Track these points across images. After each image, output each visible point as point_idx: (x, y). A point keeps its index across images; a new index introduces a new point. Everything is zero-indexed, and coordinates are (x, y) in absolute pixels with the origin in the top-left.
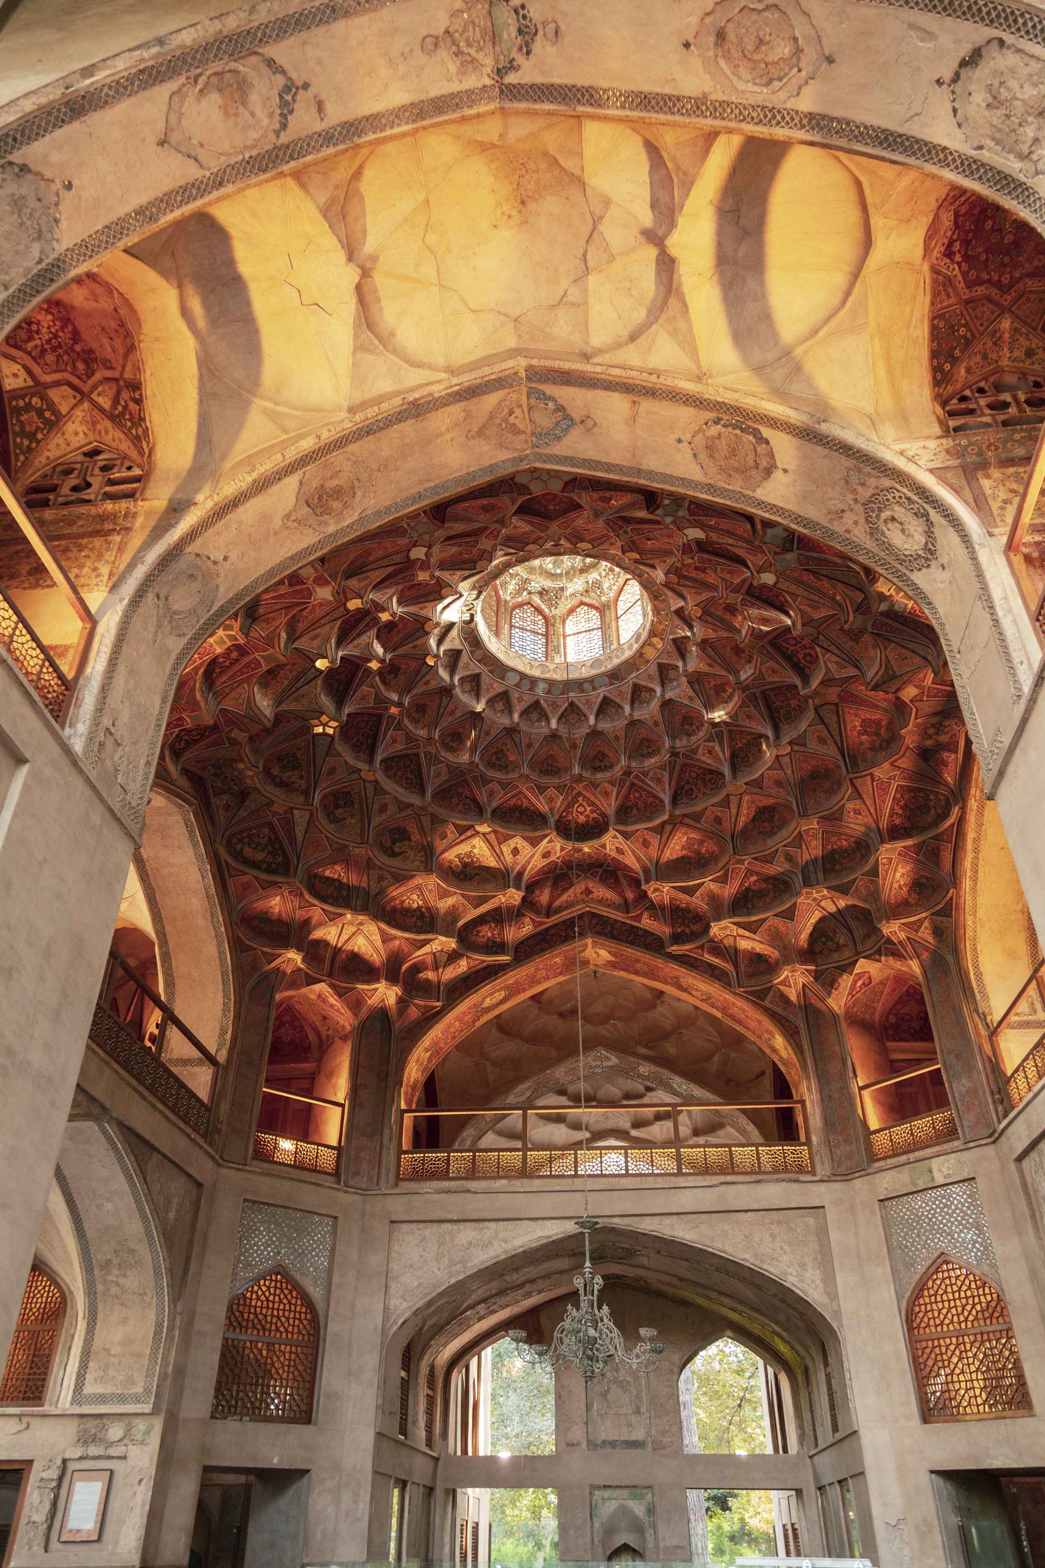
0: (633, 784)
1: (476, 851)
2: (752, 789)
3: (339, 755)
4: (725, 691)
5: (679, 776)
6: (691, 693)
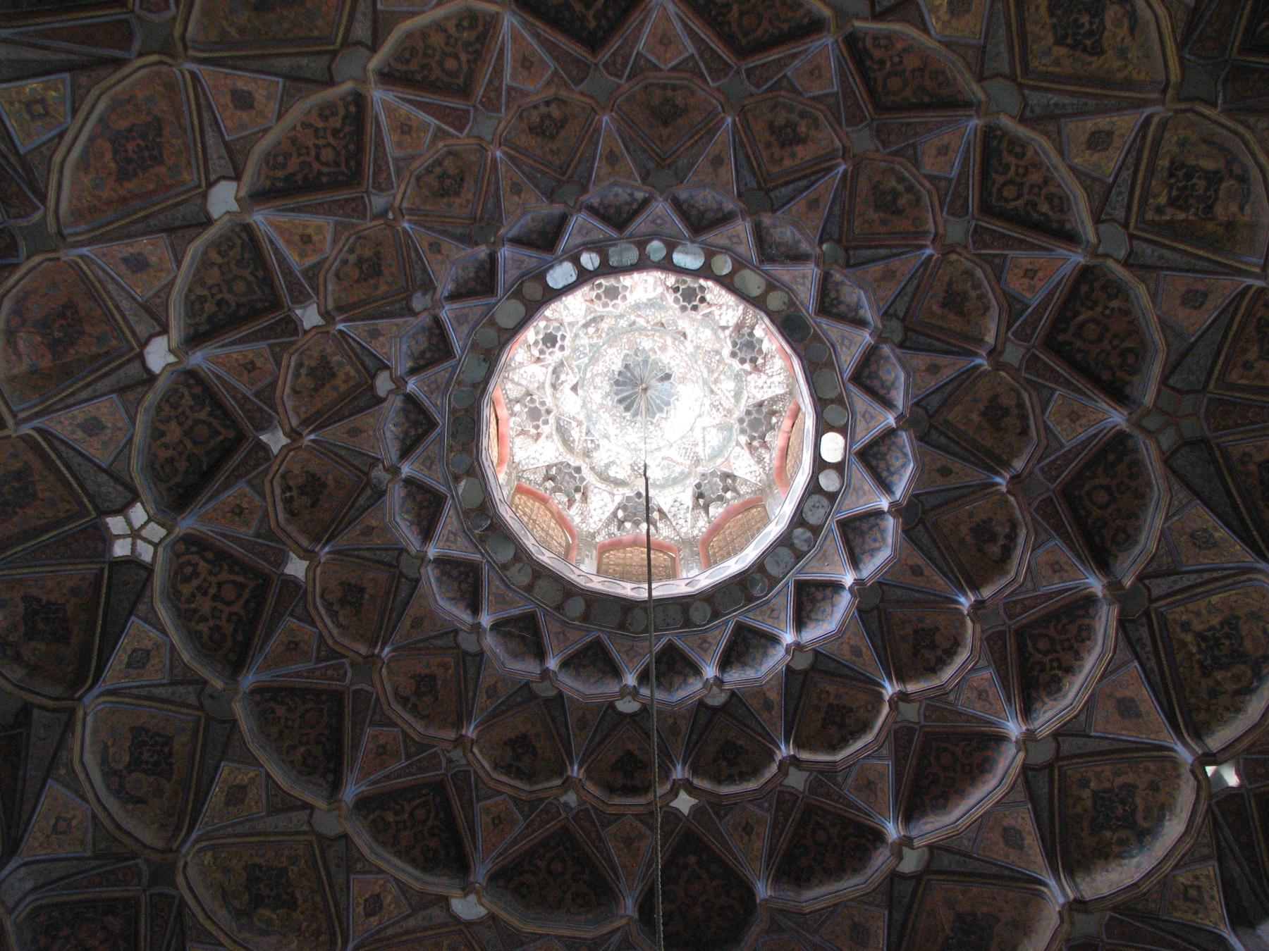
0: (465, 92)
3: (1161, 321)
4: (312, 372)
5: (360, 149)
6: (377, 347)
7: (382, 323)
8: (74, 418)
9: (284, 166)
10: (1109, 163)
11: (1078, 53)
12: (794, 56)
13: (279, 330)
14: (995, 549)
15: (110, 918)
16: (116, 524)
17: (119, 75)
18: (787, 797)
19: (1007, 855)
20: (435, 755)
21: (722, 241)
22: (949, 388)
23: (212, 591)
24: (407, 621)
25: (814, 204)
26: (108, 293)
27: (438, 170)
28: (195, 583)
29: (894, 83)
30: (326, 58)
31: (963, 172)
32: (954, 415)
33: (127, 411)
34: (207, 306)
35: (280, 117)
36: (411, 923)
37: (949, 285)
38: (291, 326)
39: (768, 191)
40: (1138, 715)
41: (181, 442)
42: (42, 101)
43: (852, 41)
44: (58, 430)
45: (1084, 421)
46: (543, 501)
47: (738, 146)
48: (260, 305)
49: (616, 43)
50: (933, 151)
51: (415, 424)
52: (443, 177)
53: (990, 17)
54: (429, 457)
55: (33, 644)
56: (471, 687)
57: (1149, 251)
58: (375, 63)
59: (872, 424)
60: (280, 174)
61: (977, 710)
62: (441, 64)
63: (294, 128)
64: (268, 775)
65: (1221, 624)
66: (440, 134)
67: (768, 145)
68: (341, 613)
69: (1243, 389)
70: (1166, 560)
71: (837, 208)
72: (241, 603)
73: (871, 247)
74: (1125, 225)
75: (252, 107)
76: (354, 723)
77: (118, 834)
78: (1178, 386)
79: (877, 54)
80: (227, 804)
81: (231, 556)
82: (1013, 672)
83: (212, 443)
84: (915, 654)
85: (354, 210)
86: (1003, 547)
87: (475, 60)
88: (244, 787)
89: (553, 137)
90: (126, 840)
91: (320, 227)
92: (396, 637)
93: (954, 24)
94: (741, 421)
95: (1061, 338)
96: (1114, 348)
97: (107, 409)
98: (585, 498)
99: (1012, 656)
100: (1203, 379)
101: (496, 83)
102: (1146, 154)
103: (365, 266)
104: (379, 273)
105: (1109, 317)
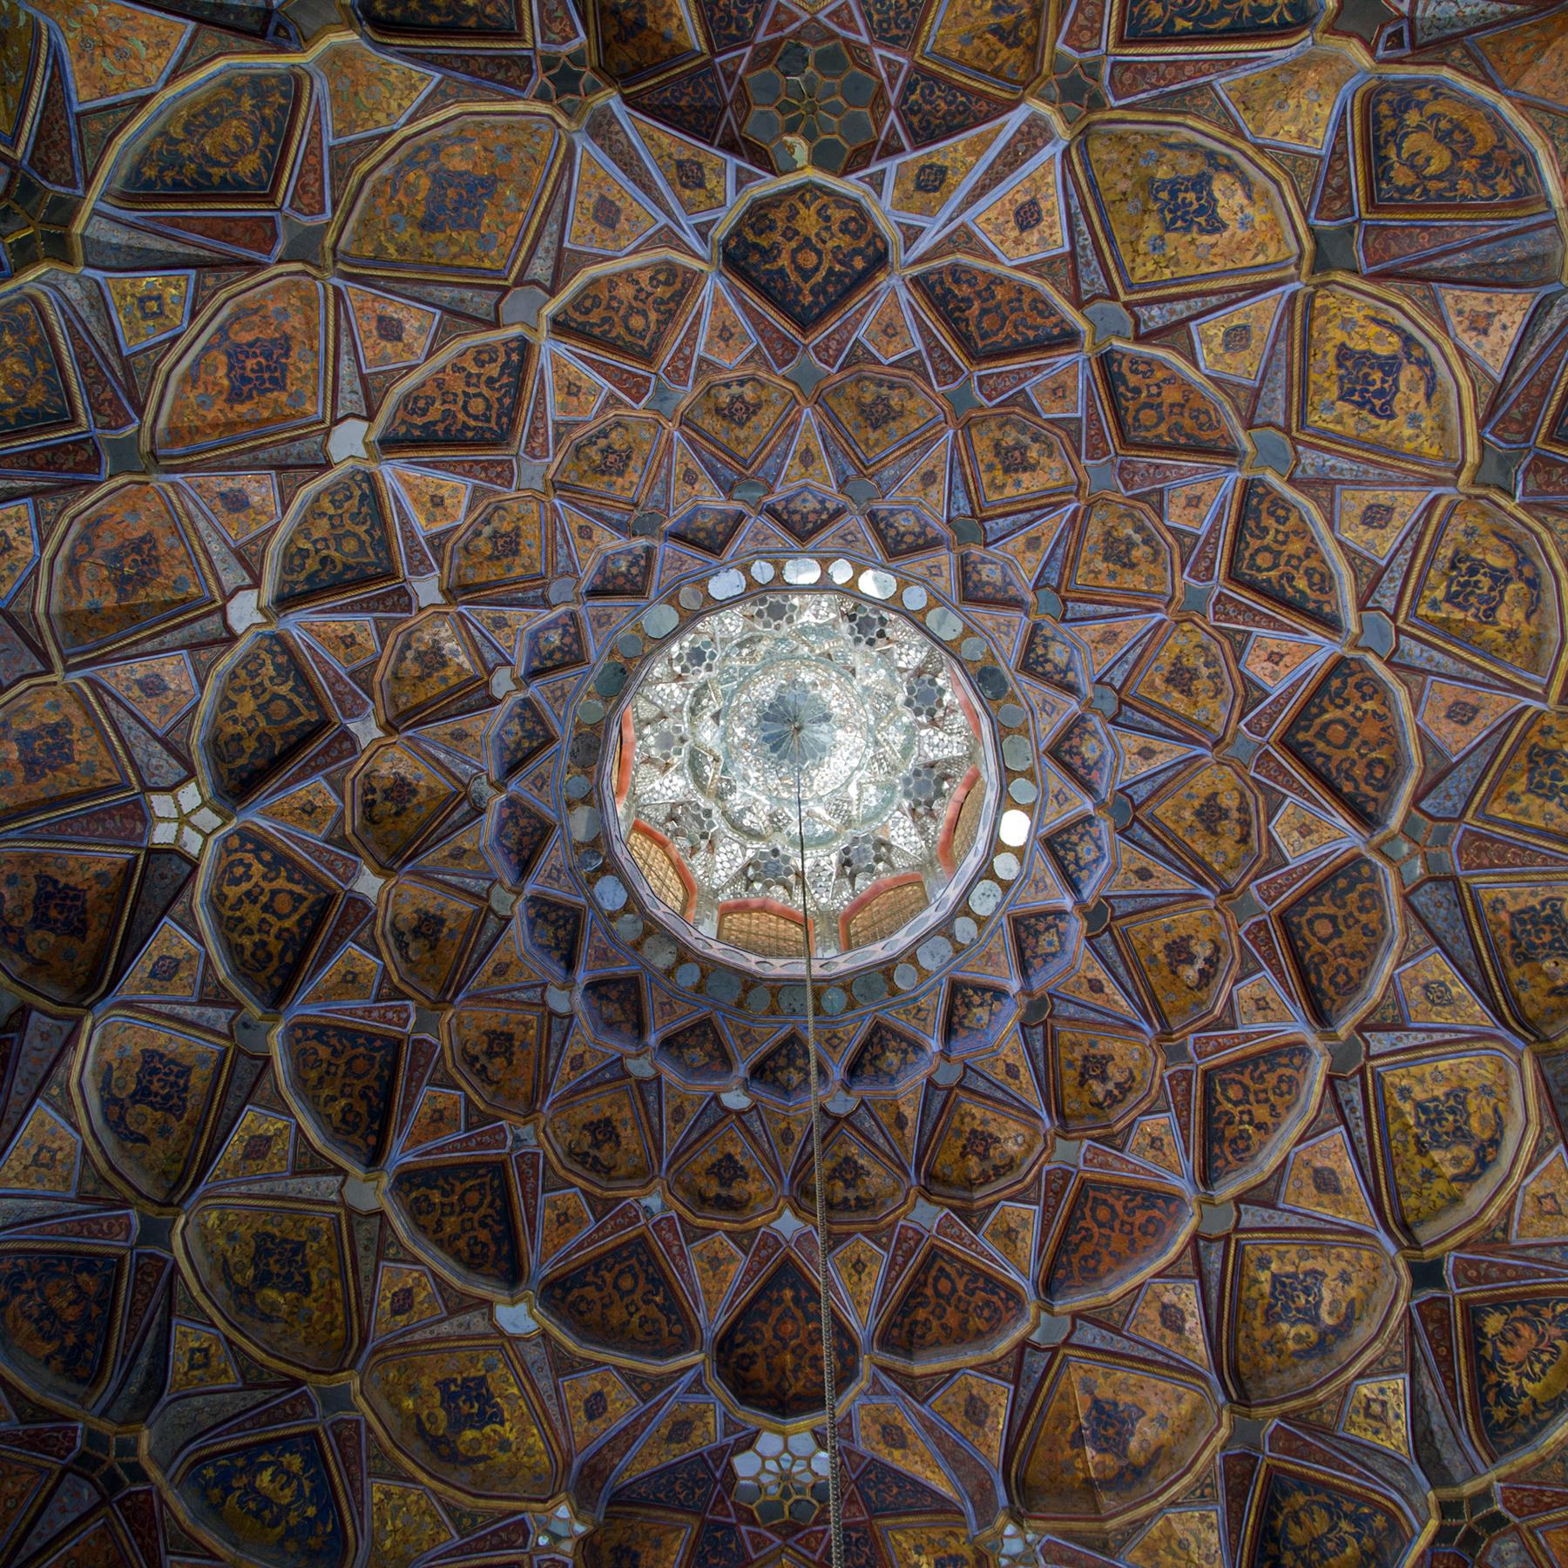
0: (647, 357)
1: (1152, 227)
2: (308, 447)
3: (1422, 735)
4: (420, 656)
5: (517, 403)
6: (500, 638)
7: (511, 613)
8: (132, 671)
9: (424, 412)
10: (1383, 543)
11: (1365, 413)
12: (1037, 369)
13: (389, 603)
14: (1190, 973)
15: (84, 1277)
16: (161, 804)
17: (251, 281)
18: (910, 1234)
19: (1163, 1337)
20: (502, 1128)
21: (920, 570)
22: (1162, 778)
23: (264, 899)
24: (489, 966)
25: (1033, 543)
26: (196, 530)
27: (602, 443)
28: (245, 886)
29: (1147, 416)
30: (496, 294)
31: (1213, 529)
32: (1163, 810)
33: (196, 673)
34: (309, 562)
35: (430, 354)
36: (445, 1328)
37: (1178, 658)
38: (402, 600)
39: (983, 520)
40: (1337, 1191)
41: (252, 717)
42: (159, 298)
43: (1106, 361)
44: (111, 684)
45: (1315, 837)
46: (662, 844)
47: (955, 464)
48: (371, 571)
49: (833, 323)
50: (1183, 502)
51: (530, 735)
52: (608, 450)
53: (1270, 359)
54: (541, 776)
55: (39, 934)
56: (554, 1054)
57: (1417, 651)
58: (552, 307)
59: (1065, 807)
60: (419, 421)
61: (1146, 1160)
62: (625, 320)
63: (443, 370)
64: (298, 1127)
65: (1447, 1095)
66: (611, 402)
67: (990, 468)
68: (413, 945)
69: (1505, 824)
70: (1390, 1012)
71: (1060, 551)
72: (296, 917)
73: (1092, 602)
74: (1394, 618)
75: (399, 339)
76: (410, 1079)
77: (111, 1177)
78: (1432, 811)
79: (1133, 380)
80: (246, 1156)
81: (293, 861)
82: (1196, 1118)
83: (290, 724)
84: (1082, 1084)
85: (498, 475)
86: (1201, 971)
87: (666, 322)
88: (269, 1139)
89: (741, 424)
90: (120, 1185)
91: (455, 489)
92: (473, 985)
93: (1228, 358)
94: (907, 781)
95: (1301, 736)
96: (1362, 756)
97: (174, 670)
98: (712, 847)
99: (1196, 1103)
100: (1460, 807)
101: (687, 351)
102: (1428, 539)
103: (500, 542)
104: (516, 553)
105: (1360, 720)
